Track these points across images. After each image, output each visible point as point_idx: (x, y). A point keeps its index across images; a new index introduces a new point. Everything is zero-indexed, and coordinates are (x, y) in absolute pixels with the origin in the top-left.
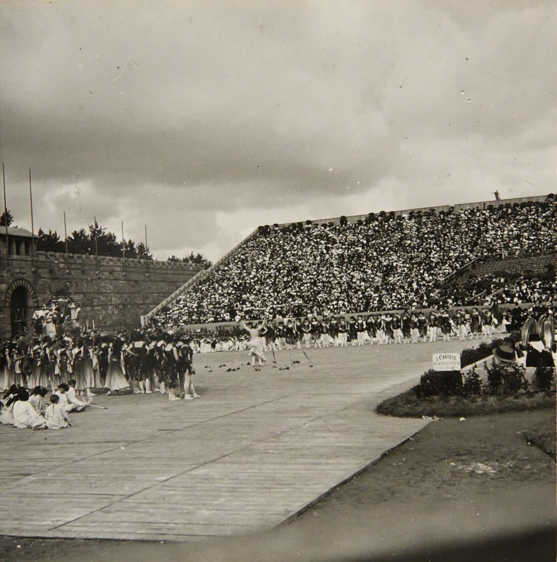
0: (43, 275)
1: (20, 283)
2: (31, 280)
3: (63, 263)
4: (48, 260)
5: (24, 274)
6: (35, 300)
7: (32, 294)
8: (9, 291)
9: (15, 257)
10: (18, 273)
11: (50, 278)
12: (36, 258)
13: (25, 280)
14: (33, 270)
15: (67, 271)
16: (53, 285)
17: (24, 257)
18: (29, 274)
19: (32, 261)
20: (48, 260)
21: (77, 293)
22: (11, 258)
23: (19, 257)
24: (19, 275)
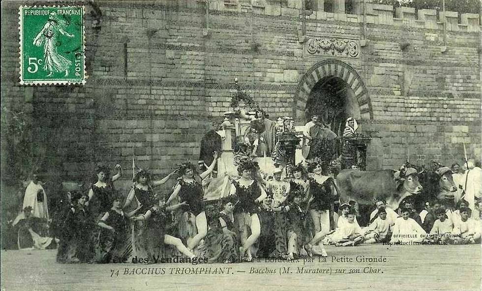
0: (384, 55)
1: (329, 70)
2: (355, 63)
3: (435, 31)
4: (397, 24)
5: (341, 51)
6: (366, 106)
7: (357, 93)
8: (305, 86)
9: (321, 15)
10: (326, 49)
11: (402, 62)
12: (370, 19)
13: (344, 65)
14: (363, 42)
15: (444, 49)
16: (409, 77)
17: (342, 16)
18: (351, 51)
19: (361, 24)
20: (397, 24)
21: (467, 96)
22: (313, 17)
23: (330, 14)
24: (330, 52)
